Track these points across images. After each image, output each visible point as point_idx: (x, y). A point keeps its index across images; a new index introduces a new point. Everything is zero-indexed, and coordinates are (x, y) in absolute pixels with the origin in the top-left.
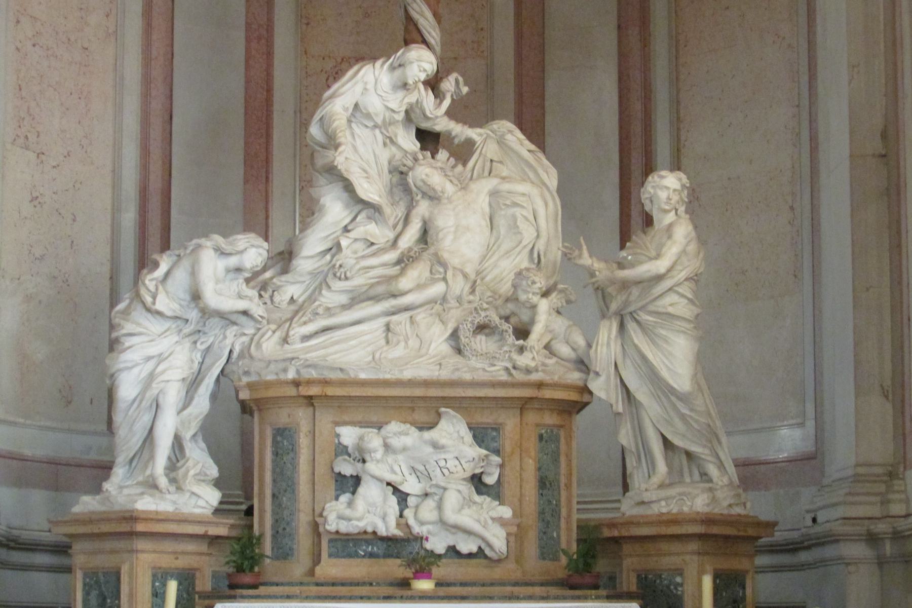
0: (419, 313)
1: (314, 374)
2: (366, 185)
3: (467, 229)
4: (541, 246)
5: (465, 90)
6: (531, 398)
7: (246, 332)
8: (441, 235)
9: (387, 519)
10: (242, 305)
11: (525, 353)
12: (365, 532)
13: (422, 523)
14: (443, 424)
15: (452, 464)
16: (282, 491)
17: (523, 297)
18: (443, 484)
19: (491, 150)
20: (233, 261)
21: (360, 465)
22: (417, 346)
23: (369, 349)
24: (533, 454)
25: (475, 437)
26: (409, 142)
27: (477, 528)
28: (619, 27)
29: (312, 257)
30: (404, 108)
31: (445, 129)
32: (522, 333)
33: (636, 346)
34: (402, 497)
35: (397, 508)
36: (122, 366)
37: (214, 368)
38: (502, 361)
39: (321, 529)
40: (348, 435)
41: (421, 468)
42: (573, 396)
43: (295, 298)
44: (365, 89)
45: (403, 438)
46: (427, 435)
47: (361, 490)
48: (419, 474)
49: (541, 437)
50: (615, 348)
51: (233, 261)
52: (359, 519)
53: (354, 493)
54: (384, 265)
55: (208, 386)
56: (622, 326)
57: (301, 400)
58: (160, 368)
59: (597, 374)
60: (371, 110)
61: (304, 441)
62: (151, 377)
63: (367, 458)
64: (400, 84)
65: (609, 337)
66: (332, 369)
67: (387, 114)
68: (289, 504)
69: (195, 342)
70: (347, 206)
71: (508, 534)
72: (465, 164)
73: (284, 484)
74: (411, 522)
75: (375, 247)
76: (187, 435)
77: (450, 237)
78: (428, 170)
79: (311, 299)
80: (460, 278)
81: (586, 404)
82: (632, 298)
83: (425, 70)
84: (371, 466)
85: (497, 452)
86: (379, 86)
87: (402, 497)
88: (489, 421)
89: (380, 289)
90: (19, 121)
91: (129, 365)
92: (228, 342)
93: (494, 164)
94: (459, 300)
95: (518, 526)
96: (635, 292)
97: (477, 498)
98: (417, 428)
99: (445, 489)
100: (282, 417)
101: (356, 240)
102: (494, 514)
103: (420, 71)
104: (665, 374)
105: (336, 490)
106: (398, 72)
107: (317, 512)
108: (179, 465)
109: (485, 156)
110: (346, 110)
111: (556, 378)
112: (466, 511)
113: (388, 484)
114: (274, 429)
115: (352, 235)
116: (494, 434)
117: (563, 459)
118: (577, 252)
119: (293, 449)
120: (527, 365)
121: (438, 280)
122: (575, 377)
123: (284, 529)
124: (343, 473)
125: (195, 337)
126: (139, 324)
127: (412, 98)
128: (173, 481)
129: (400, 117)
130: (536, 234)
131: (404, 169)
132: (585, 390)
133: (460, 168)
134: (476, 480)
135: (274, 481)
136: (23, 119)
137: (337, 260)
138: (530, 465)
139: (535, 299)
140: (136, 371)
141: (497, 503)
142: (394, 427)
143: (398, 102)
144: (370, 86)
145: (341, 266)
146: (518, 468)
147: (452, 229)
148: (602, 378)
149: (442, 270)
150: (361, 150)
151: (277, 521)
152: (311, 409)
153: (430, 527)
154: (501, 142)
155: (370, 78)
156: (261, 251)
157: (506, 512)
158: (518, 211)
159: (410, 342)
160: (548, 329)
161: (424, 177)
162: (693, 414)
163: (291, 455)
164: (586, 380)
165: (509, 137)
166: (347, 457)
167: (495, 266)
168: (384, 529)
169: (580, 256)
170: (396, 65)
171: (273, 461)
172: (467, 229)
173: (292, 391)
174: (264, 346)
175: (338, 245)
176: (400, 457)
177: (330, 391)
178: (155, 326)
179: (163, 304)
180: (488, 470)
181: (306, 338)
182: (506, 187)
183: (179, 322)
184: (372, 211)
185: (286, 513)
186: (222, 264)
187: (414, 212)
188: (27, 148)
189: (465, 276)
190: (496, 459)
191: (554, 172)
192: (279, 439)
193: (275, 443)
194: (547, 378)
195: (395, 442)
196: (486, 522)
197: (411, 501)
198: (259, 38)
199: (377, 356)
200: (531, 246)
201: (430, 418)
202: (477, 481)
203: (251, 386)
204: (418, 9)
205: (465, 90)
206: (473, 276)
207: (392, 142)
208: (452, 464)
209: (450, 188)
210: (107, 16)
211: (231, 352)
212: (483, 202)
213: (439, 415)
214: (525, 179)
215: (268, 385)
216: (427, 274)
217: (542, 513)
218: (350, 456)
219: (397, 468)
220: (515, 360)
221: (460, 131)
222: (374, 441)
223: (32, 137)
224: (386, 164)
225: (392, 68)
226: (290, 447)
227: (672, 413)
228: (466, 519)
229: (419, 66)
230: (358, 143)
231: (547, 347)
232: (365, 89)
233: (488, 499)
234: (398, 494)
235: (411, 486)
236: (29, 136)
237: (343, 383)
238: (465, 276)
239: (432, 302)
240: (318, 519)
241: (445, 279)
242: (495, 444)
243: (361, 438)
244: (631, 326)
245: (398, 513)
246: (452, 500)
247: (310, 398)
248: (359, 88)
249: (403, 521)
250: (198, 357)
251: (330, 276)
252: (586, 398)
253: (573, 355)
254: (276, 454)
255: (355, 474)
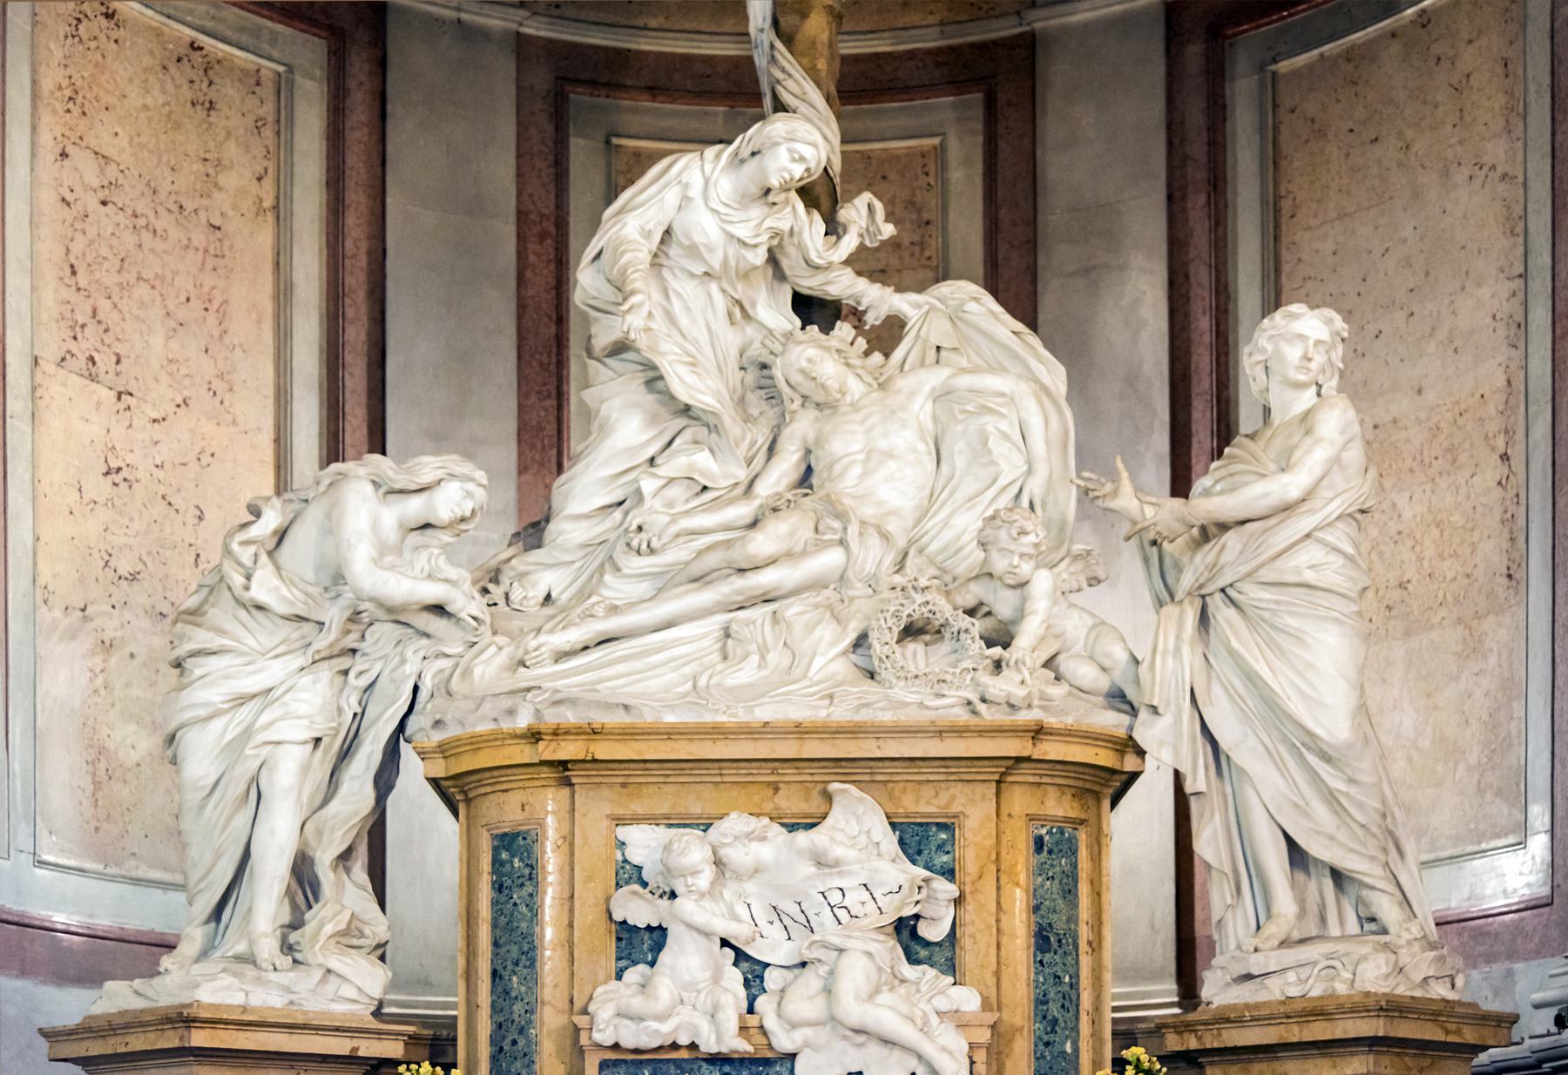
0: (790, 605)
1: (570, 717)
2: (690, 379)
3: (890, 455)
4: (1035, 487)
5: (888, 230)
6: (1019, 760)
7: (447, 650)
8: (837, 469)
9: (720, 1016)
10: (433, 592)
11: (1005, 672)
12: (674, 1046)
13: (794, 1026)
14: (837, 814)
15: (855, 898)
16: (510, 966)
17: (1000, 564)
18: (836, 941)
19: (939, 330)
20: (414, 507)
21: (665, 903)
22: (786, 662)
23: (687, 670)
24: (1022, 878)
25: (902, 842)
26: (776, 314)
27: (906, 1032)
28: (1170, 198)
29: (586, 516)
30: (764, 238)
31: (848, 292)
32: (1001, 638)
33: (1232, 653)
34: (754, 973)
35: (742, 993)
36: (187, 715)
37: (380, 723)
38: (958, 688)
39: (584, 1040)
40: (643, 843)
41: (793, 909)
42: (1104, 757)
43: (554, 594)
44: (685, 199)
45: (755, 845)
46: (802, 837)
47: (665, 957)
48: (788, 922)
49: (1039, 843)
50: (1190, 656)
51: (414, 507)
52: (661, 1018)
53: (652, 964)
54: (727, 528)
55: (369, 757)
56: (1204, 619)
57: (546, 773)
58: (265, 718)
59: (1154, 710)
60: (698, 239)
61: (551, 861)
62: (247, 733)
63: (680, 889)
64: (755, 190)
65: (1178, 638)
66: (608, 706)
67: (732, 250)
68: (523, 989)
69: (345, 673)
70: (653, 419)
71: (972, 1046)
72: (887, 355)
73: (514, 949)
74: (771, 1023)
75: (708, 496)
76: (324, 859)
77: (857, 470)
78: (811, 352)
79: (584, 594)
80: (874, 541)
81: (1134, 776)
82: (1226, 558)
83: (802, 159)
84: (686, 906)
85: (949, 873)
86: (712, 193)
87: (754, 973)
88: (932, 809)
89: (713, 560)
90: (72, 328)
91: (202, 712)
92: (410, 669)
93: (943, 353)
94: (872, 584)
95: (993, 1027)
96: (1232, 539)
97: (909, 971)
98: (783, 825)
99: (841, 951)
100: (506, 810)
101: (671, 481)
102: (942, 1004)
103: (794, 160)
104: (1297, 707)
105: (619, 959)
106: (753, 164)
107: (578, 1005)
108: (308, 916)
109: (926, 341)
110: (648, 235)
111: (1069, 721)
112: (885, 997)
113: (725, 943)
114: (494, 837)
115: (667, 469)
116: (944, 836)
117: (1084, 889)
118: (1108, 487)
119: (532, 874)
120: (1009, 694)
121: (829, 544)
122: (1112, 721)
123: (514, 1042)
124: (631, 922)
125: (345, 662)
126: (221, 632)
127: (782, 221)
128: (288, 948)
129: (759, 257)
130: (1025, 468)
131: (768, 359)
132: (1129, 745)
133: (877, 357)
134: (906, 933)
135: (496, 944)
136: (83, 326)
137: (634, 518)
138: (1018, 900)
139: (1026, 568)
140: (217, 725)
141: (951, 979)
142: (736, 823)
143: (754, 226)
144: (695, 192)
145: (640, 528)
146: (993, 907)
147: (861, 457)
148: (1166, 721)
149: (837, 525)
150: (683, 321)
151: (500, 1026)
152: (566, 791)
153: (807, 1032)
154: (955, 318)
155: (695, 178)
156: (471, 486)
157: (968, 999)
158: (991, 424)
159: (772, 657)
160: (1050, 632)
161: (804, 364)
162: (1353, 791)
163: (529, 889)
164: (1131, 728)
165: (972, 307)
166: (637, 887)
167: (945, 524)
168: (713, 1039)
169: (1115, 493)
170: (746, 153)
171: (495, 903)
172: (890, 455)
173: (523, 753)
174: (478, 671)
175: (639, 496)
176: (750, 887)
177: (603, 751)
178: (256, 636)
179: (266, 586)
180: (927, 911)
181: (562, 656)
182: (966, 381)
183: (307, 628)
184: (705, 430)
185: (518, 1008)
186: (392, 515)
187: (786, 433)
188: (93, 378)
189: (885, 537)
190: (945, 889)
191: (1061, 370)
192: (504, 855)
193: (497, 863)
194: (1051, 721)
195: (737, 855)
196: (926, 1022)
197: (772, 979)
198: (543, 236)
199: (702, 682)
200: (1014, 490)
201: (815, 805)
202: (906, 930)
203: (445, 750)
204: (796, 89)
205: (888, 230)
206: (901, 543)
207: (746, 315)
208: (855, 898)
209: (855, 387)
210: (259, 179)
211: (416, 689)
212: (922, 410)
213: (828, 797)
214: (996, 369)
215: (476, 743)
216: (808, 533)
217: (1042, 1001)
218: (645, 885)
219: (742, 911)
220: (987, 686)
221: (879, 300)
222: (693, 851)
223: (105, 362)
224: (734, 352)
225: (738, 161)
226: (527, 871)
227: (1308, 791)
228: (886, 1015)
229: (790, 150)
230: (676, 305)
231: (1048, 664)
232: (685, 199)
233: (931, 972)
234: (745, 965)
235: (773, 948)
236: (97, 357)
237: (628, 734)
238: (885, 537)
239: (815, 585)
240: (581, 1021)
241: (842, 542)
242: (945, 858)
243: (667, 848)
244: (1223, 614)
245: (745, 1005)
246: (855, 974)
247: (563, 765)
248: (672, 196)
249: (752, 1021)
250: (351, 705)
251: (621, 546)
252: (1130, 763)
253: (1104, 683)
254: (499, 887)
255: (655, 924)
